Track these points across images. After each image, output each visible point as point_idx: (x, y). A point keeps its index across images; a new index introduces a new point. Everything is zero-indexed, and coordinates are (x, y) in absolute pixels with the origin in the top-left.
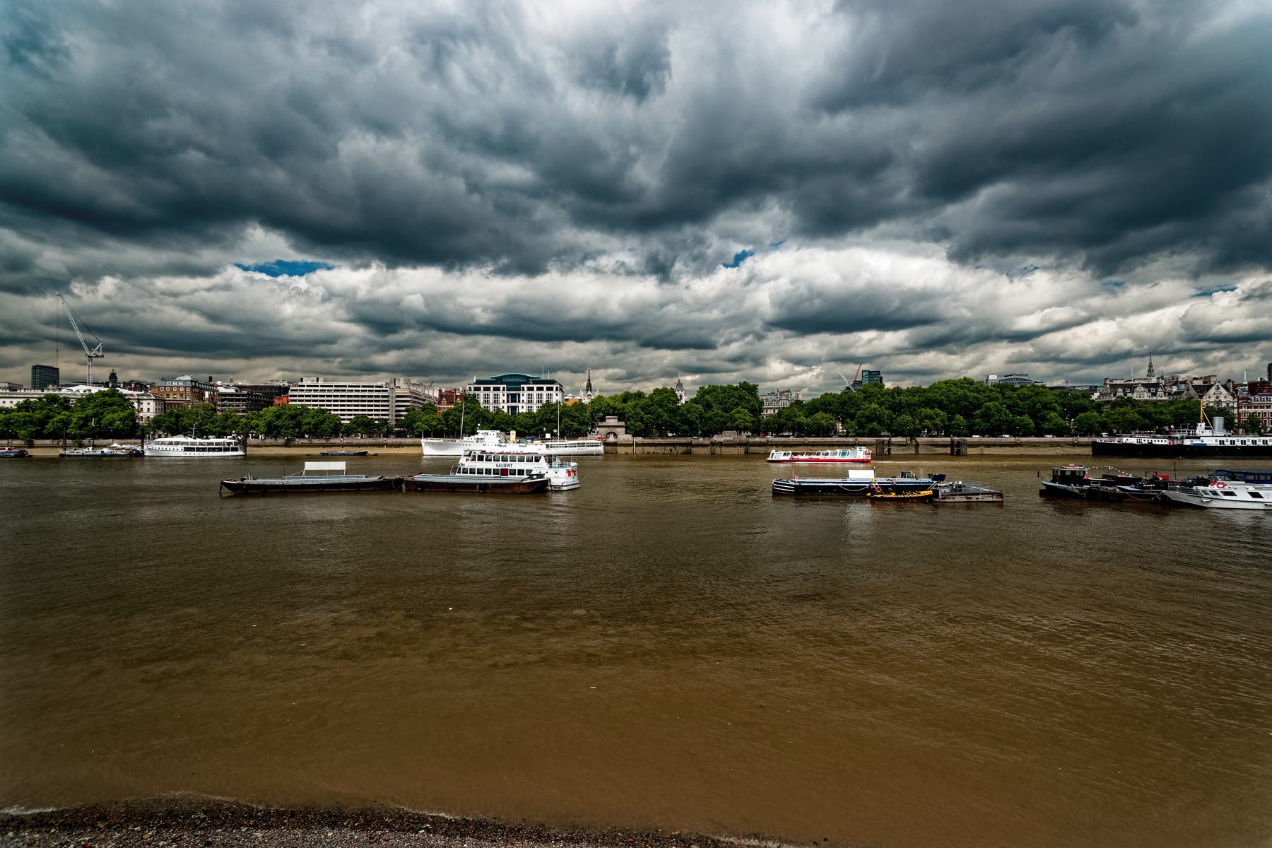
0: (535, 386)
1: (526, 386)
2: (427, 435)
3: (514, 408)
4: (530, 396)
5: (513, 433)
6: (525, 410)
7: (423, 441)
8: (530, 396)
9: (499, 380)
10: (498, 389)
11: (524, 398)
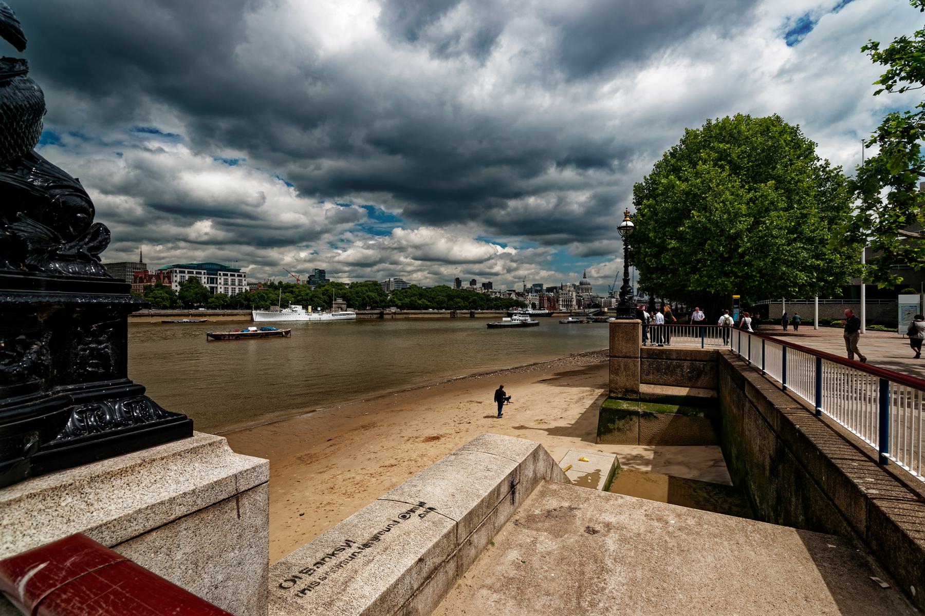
0: (229, 273)
1: (222, 273)
2: (256, 309)
3: (212, 288)
4: (226, 280)
5: (310, 307)
6: (222, 291)
7: (254, 312)
8: (226, 280)
9: (199, 266)
10: (200, 273)
11: (221, 280)
